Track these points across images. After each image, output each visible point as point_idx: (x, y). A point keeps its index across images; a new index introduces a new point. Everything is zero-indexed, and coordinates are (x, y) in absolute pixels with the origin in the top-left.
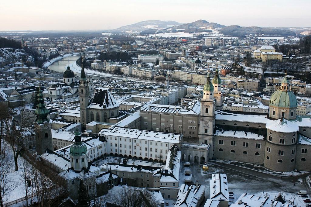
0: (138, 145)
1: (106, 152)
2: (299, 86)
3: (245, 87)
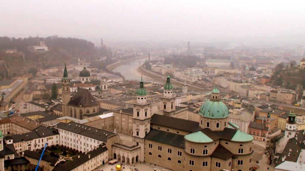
1: (58, 143)
3: (277, 97)
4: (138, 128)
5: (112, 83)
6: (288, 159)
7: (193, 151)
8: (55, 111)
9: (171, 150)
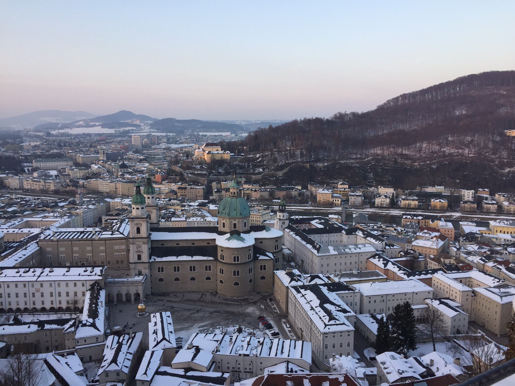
0: (38, 291)
2: (252, 190)
3: (187, 196)
4: (138, 250)
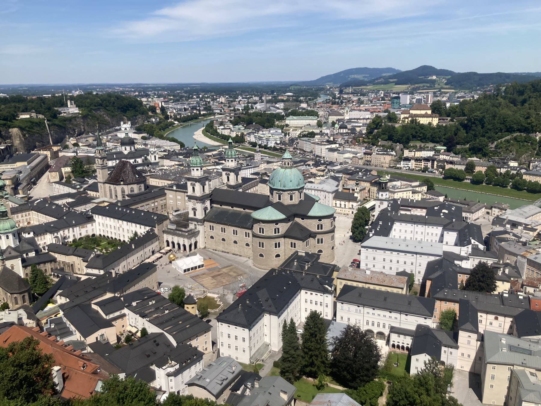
3: (372, 161)
5: (166, 152)
6: (377, 234)
7: (262, 230)
8: (89, 192)
9: (236, 231)
